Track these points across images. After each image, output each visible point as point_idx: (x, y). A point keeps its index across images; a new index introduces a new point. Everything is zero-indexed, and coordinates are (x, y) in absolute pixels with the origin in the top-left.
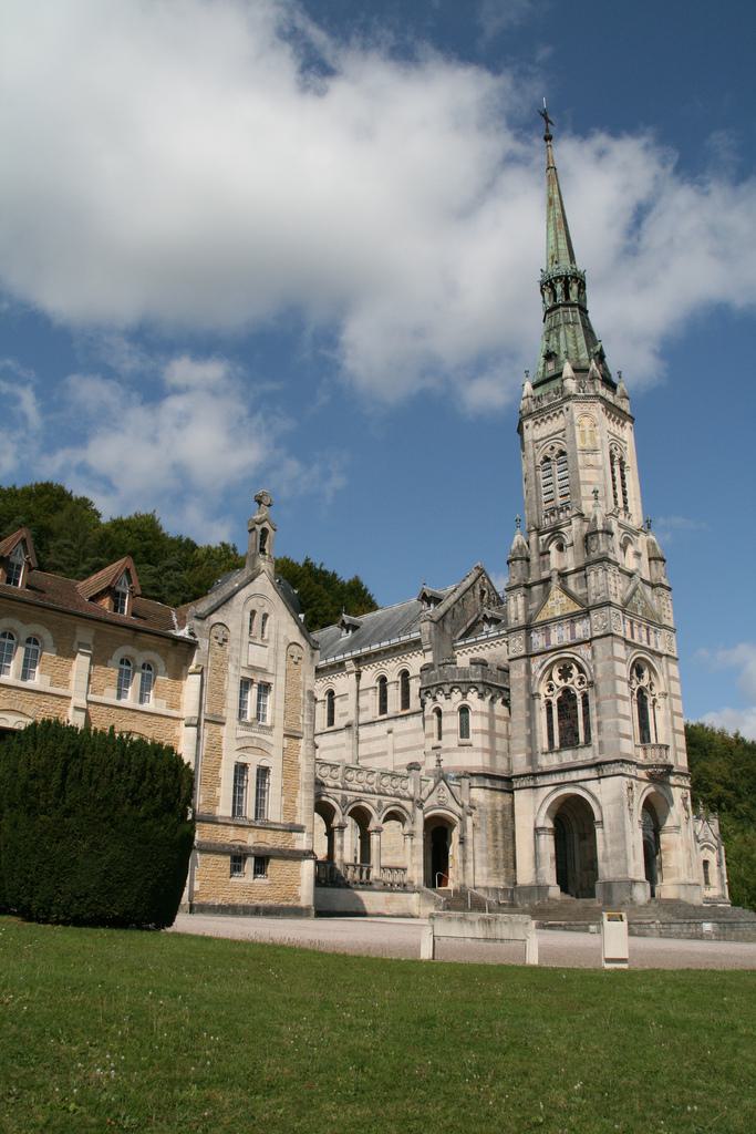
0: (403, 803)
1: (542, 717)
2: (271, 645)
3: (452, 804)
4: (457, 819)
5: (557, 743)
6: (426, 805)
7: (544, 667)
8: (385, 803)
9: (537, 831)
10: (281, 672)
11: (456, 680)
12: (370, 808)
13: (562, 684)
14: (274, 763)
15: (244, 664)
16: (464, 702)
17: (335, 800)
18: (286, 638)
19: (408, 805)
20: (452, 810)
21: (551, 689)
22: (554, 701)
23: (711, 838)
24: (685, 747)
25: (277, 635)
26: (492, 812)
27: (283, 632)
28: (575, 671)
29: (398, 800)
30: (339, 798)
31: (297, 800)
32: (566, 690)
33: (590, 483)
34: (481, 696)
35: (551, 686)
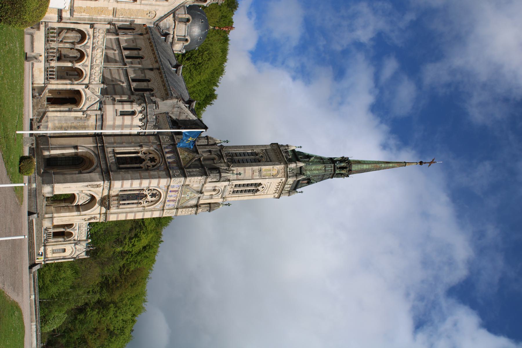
0: (87, 78)
1: (132, 149)
3: (88, 104)
4: (81, 107)
5: (119, 156)
6: (87, 90)
7: (155, 150)
8: (86, 68)
9: (76, 147)
10: (142, 7)
11: (148, 109)
13: (148, 158)
16: (137, 113)
18: (158, 10)
19: (86, 81)
20: (84, 104)
21: (145, 153)
22: (139, 155)
23: (78, 253)
24: (119, 219)
25: (159, 5)
26: (85, 125)
27: (160, 8)
28: (153, 163)
29: (89, 76)
31: (84, 14)
32: (143, 160)
33: (245, 172)
34: (141, 120)
35: (146, 154)
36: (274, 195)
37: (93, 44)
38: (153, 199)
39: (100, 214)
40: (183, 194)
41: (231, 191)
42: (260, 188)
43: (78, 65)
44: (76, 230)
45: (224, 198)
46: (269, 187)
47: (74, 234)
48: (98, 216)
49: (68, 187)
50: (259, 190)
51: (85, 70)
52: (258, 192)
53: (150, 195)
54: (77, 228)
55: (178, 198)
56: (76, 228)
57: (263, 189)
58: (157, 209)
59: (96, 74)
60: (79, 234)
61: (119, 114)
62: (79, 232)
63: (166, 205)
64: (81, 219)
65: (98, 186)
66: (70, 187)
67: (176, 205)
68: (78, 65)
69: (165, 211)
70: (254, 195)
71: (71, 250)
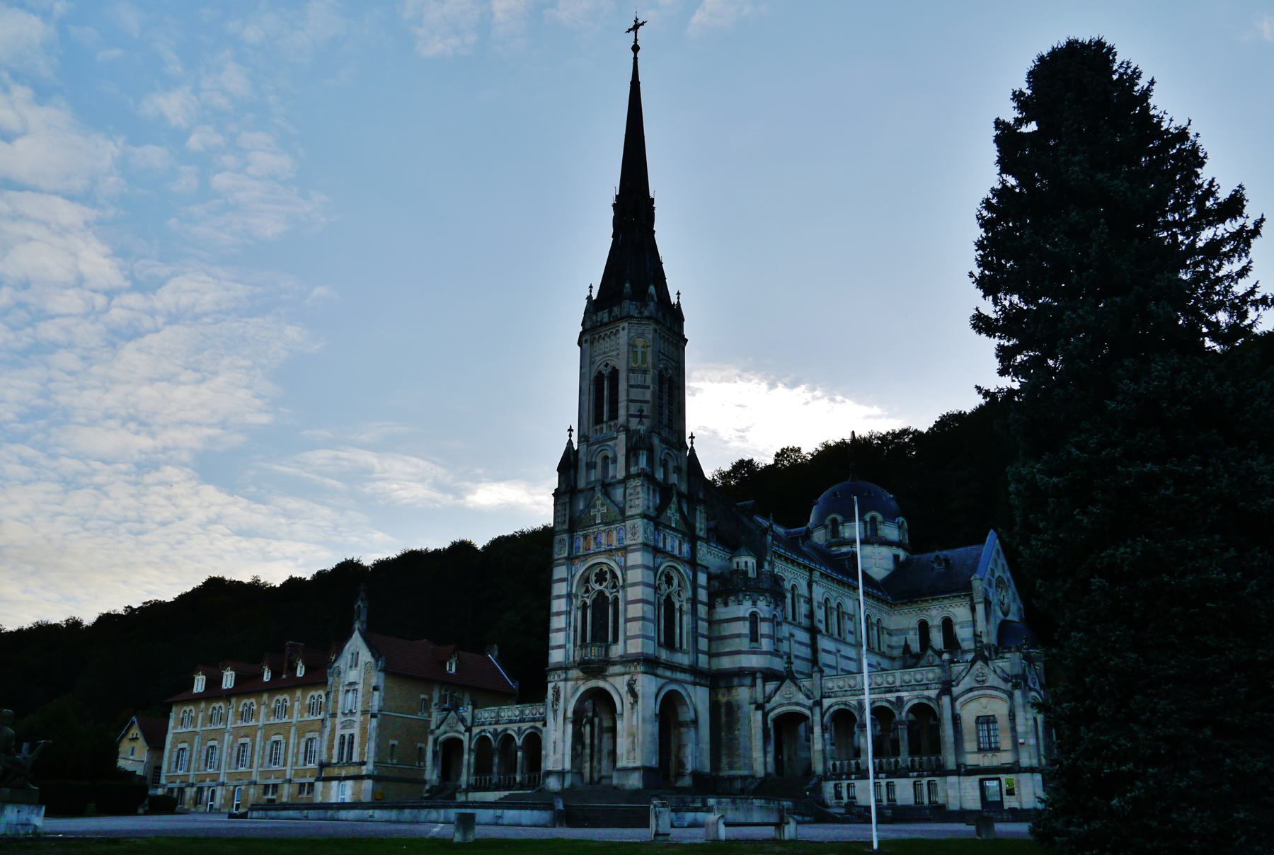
2: (359, 668)
10: (362, 681)
12: (513, 734)
14: (356, 731)
15: (346, 683)
17: (489, 732)
23: (992, 680)
30: (492, 730)
37: (490, 724)
38: (608, 576)
39: (623, 674)
42: (606, 372)
43: (519, 742)
44: (899, 698)
47: (916, 701)
48: (627, 678)
49: (555, 747)
51: (525, 731)
53: (601, 585)
54: (892, 697)
56: (893, 699)
57: (609, 362)
59: (534, 713)
60: (917, 688)
61: (754, 644)
62: (909, 688)
64: (631, 711)
65: (557, 692)
66: (555, 743)
68: (519, 742)
71: (984, 701)
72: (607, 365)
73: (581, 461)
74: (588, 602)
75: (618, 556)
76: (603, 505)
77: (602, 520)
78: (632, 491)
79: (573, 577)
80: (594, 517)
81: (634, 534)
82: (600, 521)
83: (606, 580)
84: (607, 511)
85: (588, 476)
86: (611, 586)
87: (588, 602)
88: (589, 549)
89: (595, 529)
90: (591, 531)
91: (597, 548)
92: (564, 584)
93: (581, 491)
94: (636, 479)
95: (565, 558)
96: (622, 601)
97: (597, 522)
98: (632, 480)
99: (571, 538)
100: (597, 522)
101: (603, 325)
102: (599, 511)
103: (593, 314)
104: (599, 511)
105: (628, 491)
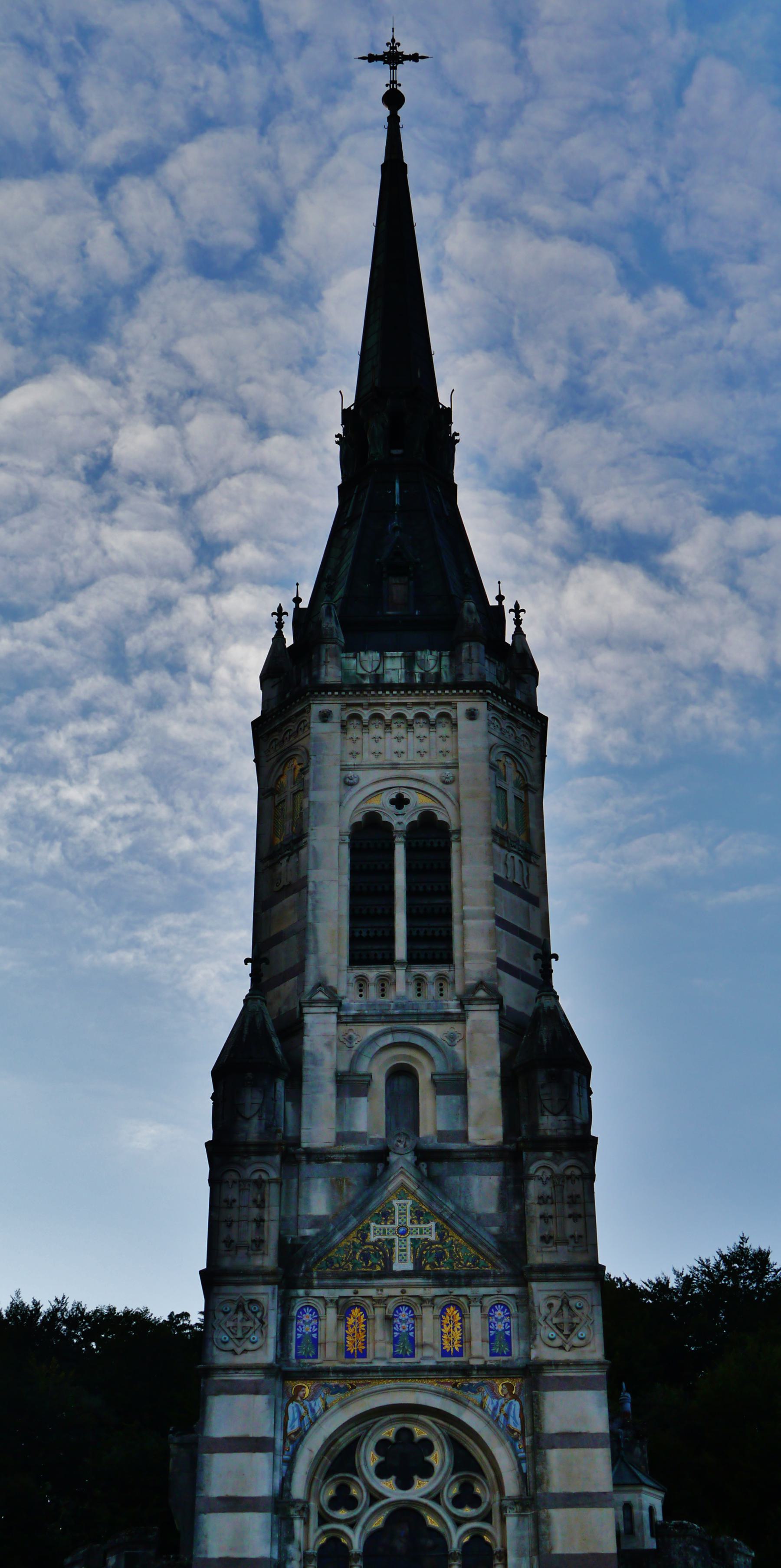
36: (464, 724)
38: (439, 1458)
40: (389, 1261)
41: (420, 981)
42: (400, 821)
45: (461, 1005)
46: (395, 766)
50: (427, 819)
52: (441, 817)
53: (405, 1484)
55: (420, 1292)
57: (407, 795)
58: (526, 1412)
63: (492, 1361)
67: (492, 1290)
69: (542, 1352)
70: (459, 832)
72: (400, 802)
73: (316, 1062)
74: (356, 1540)
75: (495, 1396)
76: (419, 1215)
77: (417, 1262)
78: (548, 1190)
79: (296, 1440)
80: (385, 1250)
81: (567, 1329)
82: (409, 1266)
83: (427, 1471)
84: (441, 1236)
85: (340, 1116)
86: (455, 1491)
87: (356, 1540)
88: (363, 1354)
89: (391, 1289)
90: (372, 1292)
91: (395, 1355)
92: (261, 1461)
93: (319, 1156)
94: (565, 1154)
95: (267, 1369)
96: (520, 1554)
97: (397, 1267)
98: (549, 1154)
99: (285, 1304)
100: (397, 1267)
101: (379, 685)
102: (403, 1231)
103: (346, 650)
104: (403, 1231)
105: (534, 1189)
